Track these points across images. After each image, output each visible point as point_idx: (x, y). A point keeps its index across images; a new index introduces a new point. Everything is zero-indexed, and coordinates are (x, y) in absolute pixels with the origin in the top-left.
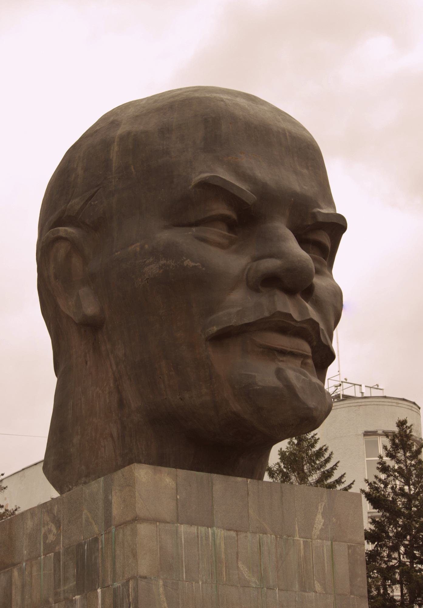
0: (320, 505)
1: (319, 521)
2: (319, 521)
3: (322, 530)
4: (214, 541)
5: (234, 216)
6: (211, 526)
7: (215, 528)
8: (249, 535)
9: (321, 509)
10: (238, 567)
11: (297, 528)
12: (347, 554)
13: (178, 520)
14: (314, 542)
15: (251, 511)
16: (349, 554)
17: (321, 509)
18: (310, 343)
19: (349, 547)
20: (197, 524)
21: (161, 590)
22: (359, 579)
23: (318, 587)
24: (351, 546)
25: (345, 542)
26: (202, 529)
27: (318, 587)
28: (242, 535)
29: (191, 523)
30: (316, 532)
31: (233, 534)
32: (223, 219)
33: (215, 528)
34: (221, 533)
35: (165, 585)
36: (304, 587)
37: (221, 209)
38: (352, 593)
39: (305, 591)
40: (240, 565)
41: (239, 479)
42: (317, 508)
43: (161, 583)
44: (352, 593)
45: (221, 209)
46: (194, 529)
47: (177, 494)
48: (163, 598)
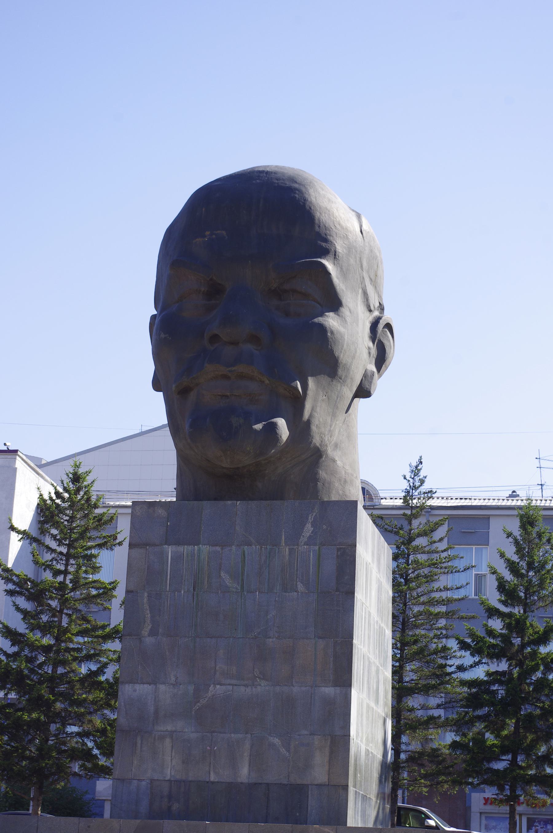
0: (310, 515)
1: (308, 529)
3: (310, 537)
4: (199, 556)
6: (198, 544)
7: (201, 546)
8: (234, 547)
9: (311, 518)
10: (220, 576)
11: (283, 538)
12: (335, 556)
14: (300, 548)
15: (237, 528)
16: (337, 556)
17: (311, 518)
19: (338, 550)
20: (184, 544)
21: (145, 600)
22: (346, 578)
23: (300, 587)
24: (340, 548)
25: (335, 545)
27: (300, 587)
29: (178, 543)
31: (218, 549)
33: (201, 546)
34: (205, 549)
35: (149, 596)
38: (337, 590)
39: (285, 592)
40: (222, 574)
41: (229, 502)
42: (307, 519)
43: (146, 594)
44: (337, 590)
47: (168, 522)
48: (146, 606)
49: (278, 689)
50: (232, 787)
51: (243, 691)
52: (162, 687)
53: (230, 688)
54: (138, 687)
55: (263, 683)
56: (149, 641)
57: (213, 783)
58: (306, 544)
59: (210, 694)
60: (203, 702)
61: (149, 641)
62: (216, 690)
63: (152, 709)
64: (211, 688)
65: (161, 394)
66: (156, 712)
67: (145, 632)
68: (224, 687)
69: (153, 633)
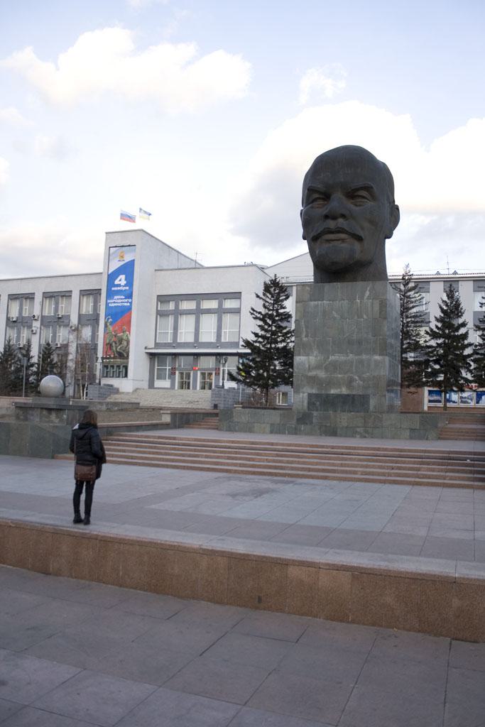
1: (367, 293)
2: (367, 293)
5: (323, 197)
6: (323, 300)
9: (368, 289)
13: (311, 301)
17: (368, 289)
23: (365, 317)
26: (320, 302)
27: (365, 317)
28: (334, 302)
29: (315, 301)
30: (365, 298)
32: (319, 198)
36: (358, 318)
37: (316, 196)
41: (335, 284)
43: (303, 321)
45: (316, 196)
46: (316, 303)
48: (304, 326)
49: (357, 357)
51: (343, 358)
52: (311, 357)
56: (305, 339)
58: (368, 299)
60: (327, 363)
61: (305, 339)
62: (332, 358)
63: (307, 366)
65: (306, 241)
66: (309, 366)
67: (304, 336)
69: (307, 336)
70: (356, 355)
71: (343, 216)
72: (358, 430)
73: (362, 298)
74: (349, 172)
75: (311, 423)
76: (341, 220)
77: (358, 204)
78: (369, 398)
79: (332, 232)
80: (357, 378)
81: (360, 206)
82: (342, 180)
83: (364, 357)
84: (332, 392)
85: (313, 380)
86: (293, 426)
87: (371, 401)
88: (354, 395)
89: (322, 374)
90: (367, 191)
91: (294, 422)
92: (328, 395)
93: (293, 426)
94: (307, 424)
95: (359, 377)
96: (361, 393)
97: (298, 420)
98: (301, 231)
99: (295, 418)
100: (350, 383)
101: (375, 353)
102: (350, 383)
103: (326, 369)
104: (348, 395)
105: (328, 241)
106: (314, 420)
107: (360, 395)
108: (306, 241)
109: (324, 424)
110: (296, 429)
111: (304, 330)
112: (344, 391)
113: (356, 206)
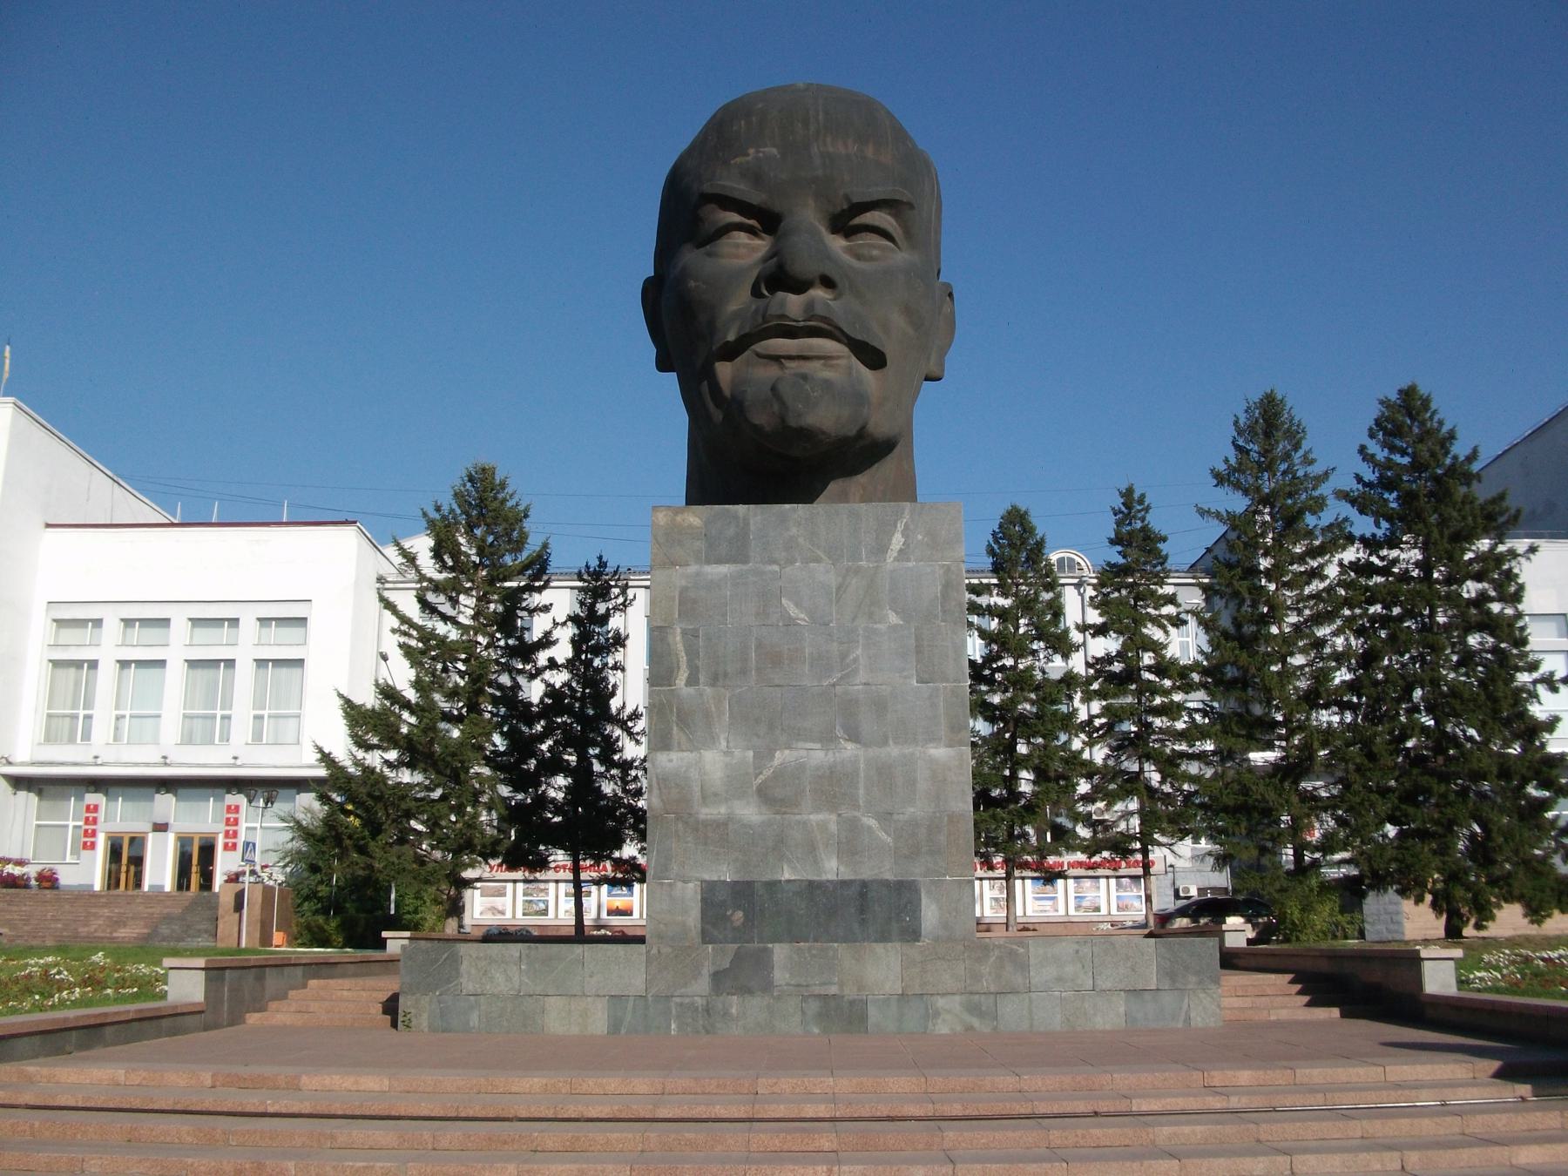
1: (897, 541)
3: (901, 551)
17: (900, 526)
18: (839, 341)
35: (684, 633)
48: (680, 647)
50: (813, 888)
53: (804, 753)
54: (674, 755)
55: (850, 746)
57: (789, 881)
59: (776, 762)
60: (767, 773)
64: (778, 754)
65: (672, 377)
68: (795, 753)
69: (692, 681)
70: (866, 745)
71: (828, 283)
72: (941, 1002)
73: (882, 549)
74: (842, 150)
75: (768, 986)
76: (818, 293)
77: (865, 251)
78: (917, 892)
79: (791, 333)
80: (872, 823)
81: (871, 259)
82: (820, 172)
83: (894, 751)
84: (787, 875)
85: (718, 835)
86: (699, 1001)
87: (924, 901)
88: (864, 884)
89: (750, 812)
90: (896, 216)
91: (702, 985)
92: (773, 885)
93: (699, 1001)
94: (750, 992)
95: (885, 817)
96: (889, 876)
97: (717, 977)
98: (652, 351)
99: (705, 972)
100: (850, 845)
101: (932, 739)
102: (850, 845)
103: (765, 795)
104: (844, 884)
105: (777, 359)
106: (780, 976)
107: (885, 884)
108: (672, 377)
109: (817, 990)
110: (708, 1010)
111: (683, 659)
112: (832, 868)
113: (858, 257)
